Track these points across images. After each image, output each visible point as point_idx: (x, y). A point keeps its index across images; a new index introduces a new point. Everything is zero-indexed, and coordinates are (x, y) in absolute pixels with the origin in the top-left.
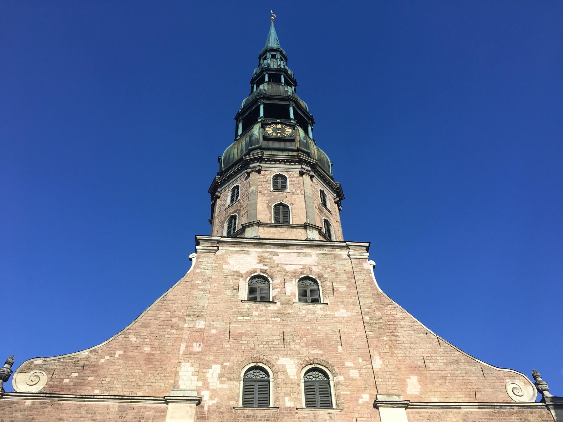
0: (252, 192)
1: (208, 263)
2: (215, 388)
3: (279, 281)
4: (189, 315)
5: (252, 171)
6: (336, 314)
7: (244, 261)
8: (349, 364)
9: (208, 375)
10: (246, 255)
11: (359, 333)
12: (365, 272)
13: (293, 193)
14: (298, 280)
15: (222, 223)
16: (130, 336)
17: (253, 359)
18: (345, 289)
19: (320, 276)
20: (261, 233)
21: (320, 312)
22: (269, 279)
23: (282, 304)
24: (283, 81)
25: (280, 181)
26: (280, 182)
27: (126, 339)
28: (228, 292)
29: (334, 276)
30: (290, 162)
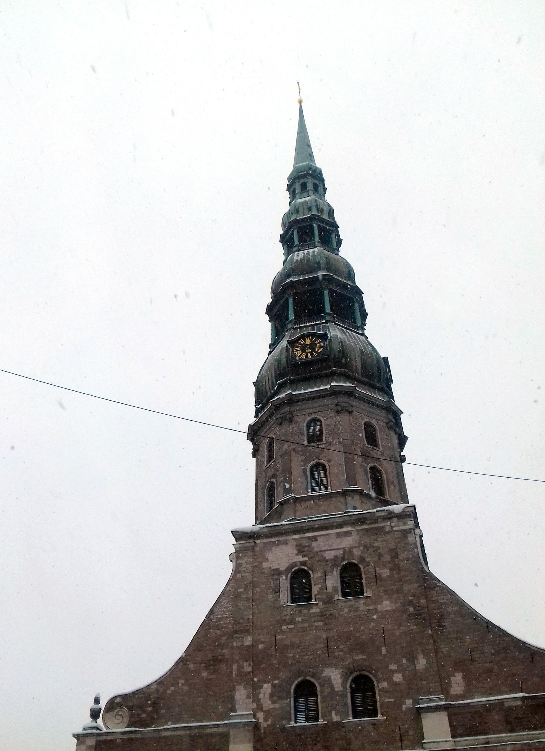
1: (247, 563)
2: (268, 709)
3: (320, 575)
4: (236, 632)
6: (379, 608)
8: (393, 667)
9: (261, 696)
11: (404, 628)
14: (339, 568)
15: (263, 488)
16: (188, 663)
17: (300, 673)
18: (388, 574)
19: (362, 560)
21: (362, 607)
22: (310, 572)
23: (324, 603)
27: (185, 667)
28: (270, 597)
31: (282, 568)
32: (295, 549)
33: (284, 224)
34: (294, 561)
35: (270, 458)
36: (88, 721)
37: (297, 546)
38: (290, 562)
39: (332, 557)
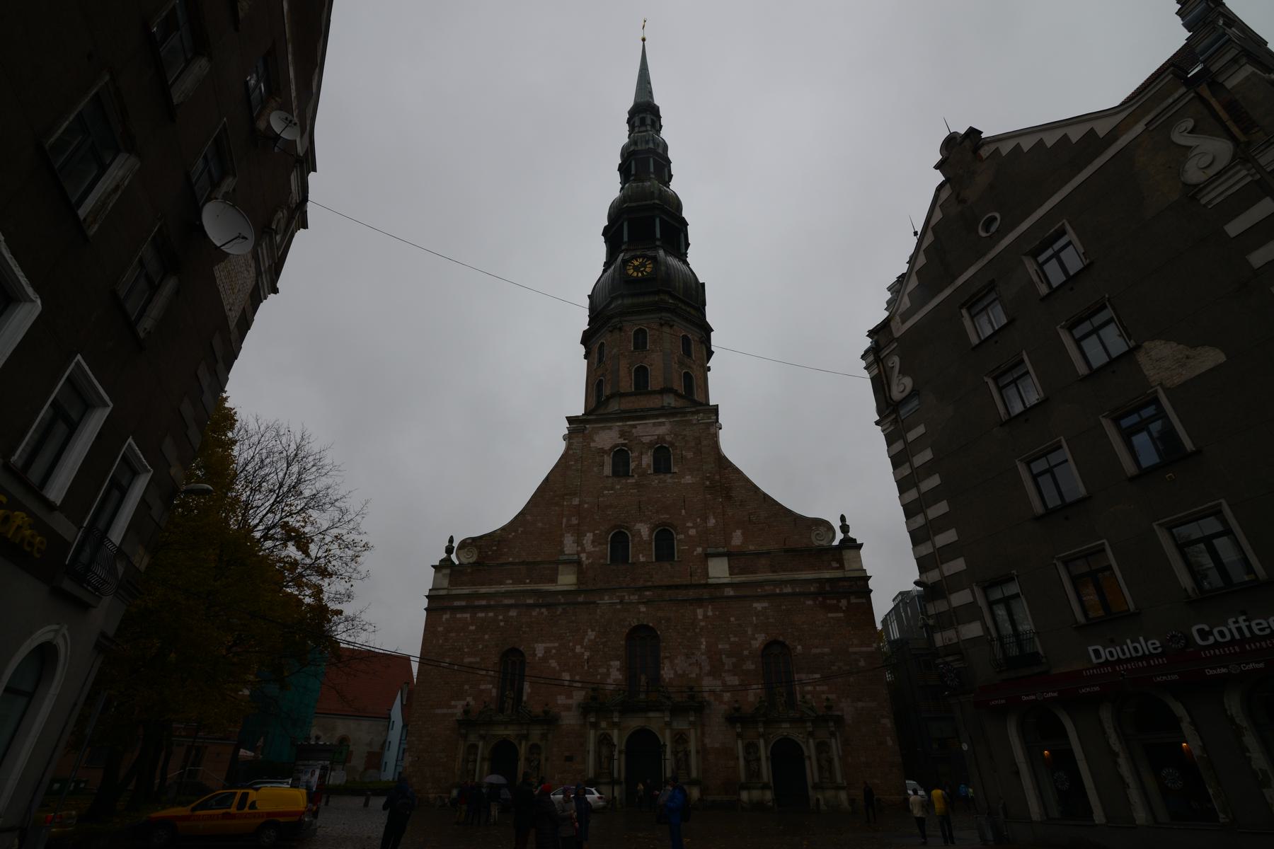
7: (607, 438)
8: (689, 524)
19: (672, 444)
26: (640, 340)
31: (607, 448)
33: (622, 155)
35: (600, 360)
36: (445, 555)
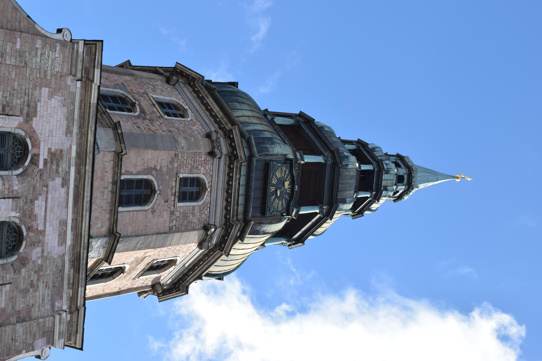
0: (176, 141)
1: (53, 60)
3: (16, 188)
5: (212, 141)
10: (64, 129)
12: (29, 341)
13: (172, 213)
14: (17, 221)
15: (123, 86)
19: (23, 262)
20: (104, 156)
22: (20, 170)
24: (362, 195)
25: (194, 189)
26: (191, 189)
29: (22, 286)
30: (227, 209)
32: (57, 147)
34: (42, 144)
37: (61, 151)
38: (41, 138)
39: (36, 211)
